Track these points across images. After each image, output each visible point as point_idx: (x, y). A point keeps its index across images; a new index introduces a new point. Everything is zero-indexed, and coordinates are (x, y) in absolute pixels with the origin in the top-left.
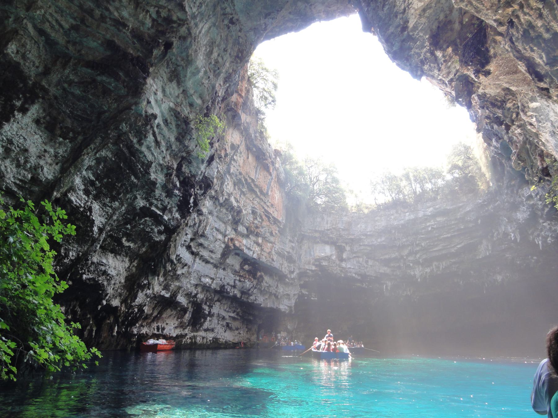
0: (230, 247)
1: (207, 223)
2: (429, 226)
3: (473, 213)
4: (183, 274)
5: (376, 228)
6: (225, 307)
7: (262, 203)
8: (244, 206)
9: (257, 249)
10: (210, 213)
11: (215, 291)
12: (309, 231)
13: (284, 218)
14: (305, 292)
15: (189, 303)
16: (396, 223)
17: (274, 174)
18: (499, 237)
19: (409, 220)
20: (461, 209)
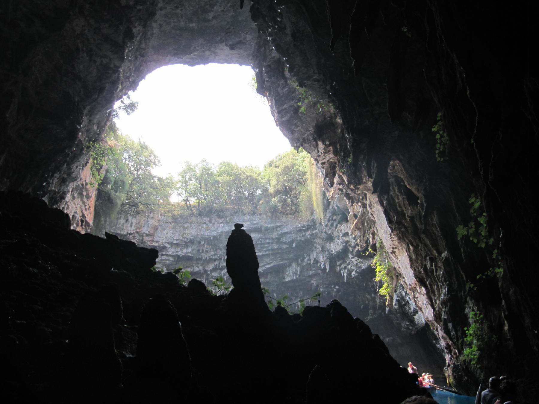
3: (289, 235)
5: (185, 236)
16: (207, 234)
19: (222, 232)
20: (278, 229)
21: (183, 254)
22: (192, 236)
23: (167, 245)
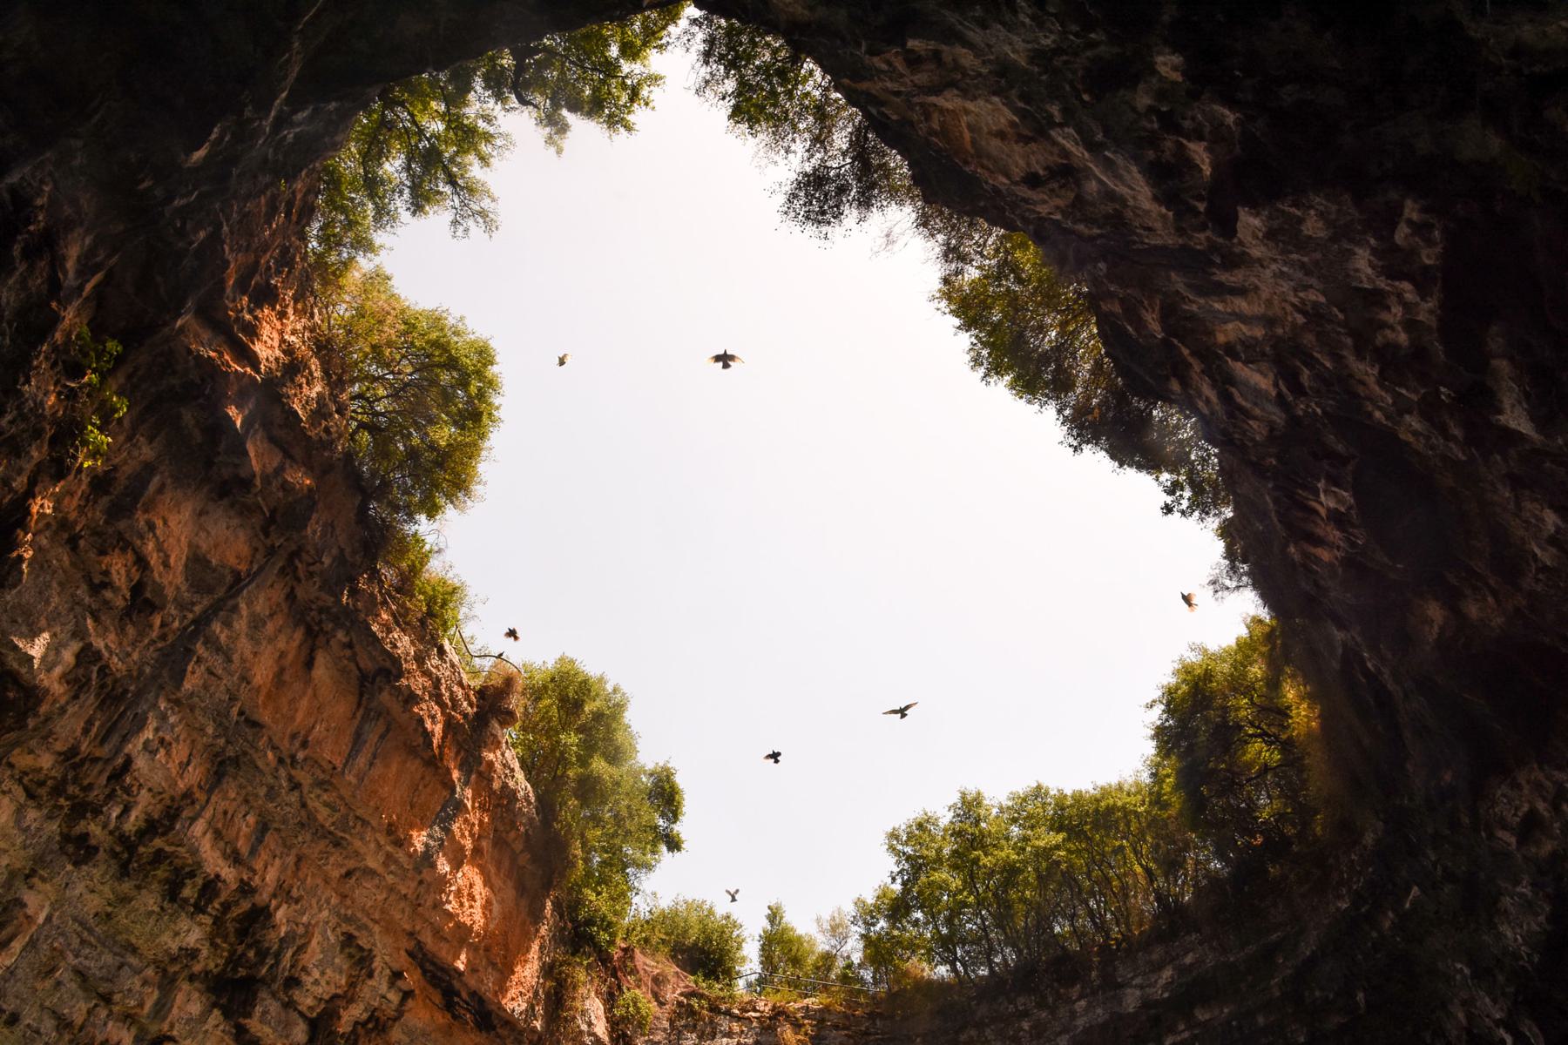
13: (539, 1009)
19: (1088, 1030)
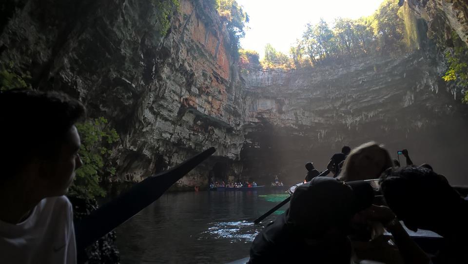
0: (186, 106)
1: (166, 87)
2: (360, 80)
4: (147, 131)
6: (182, 157)
7: (211, 66)
8: (196, 69)
9: (208, 107)
10: (168, 78)
11: (174, 144)
12: (252, 88)
13: (230, 79)
14: (249, 141)
15: (153, 155)
16: (330, 78)
17: (221, 38)
18: (421, 88)
20: (389, 64)
21: (314, 97)
22: (318, 82)
23: (300, 92)
